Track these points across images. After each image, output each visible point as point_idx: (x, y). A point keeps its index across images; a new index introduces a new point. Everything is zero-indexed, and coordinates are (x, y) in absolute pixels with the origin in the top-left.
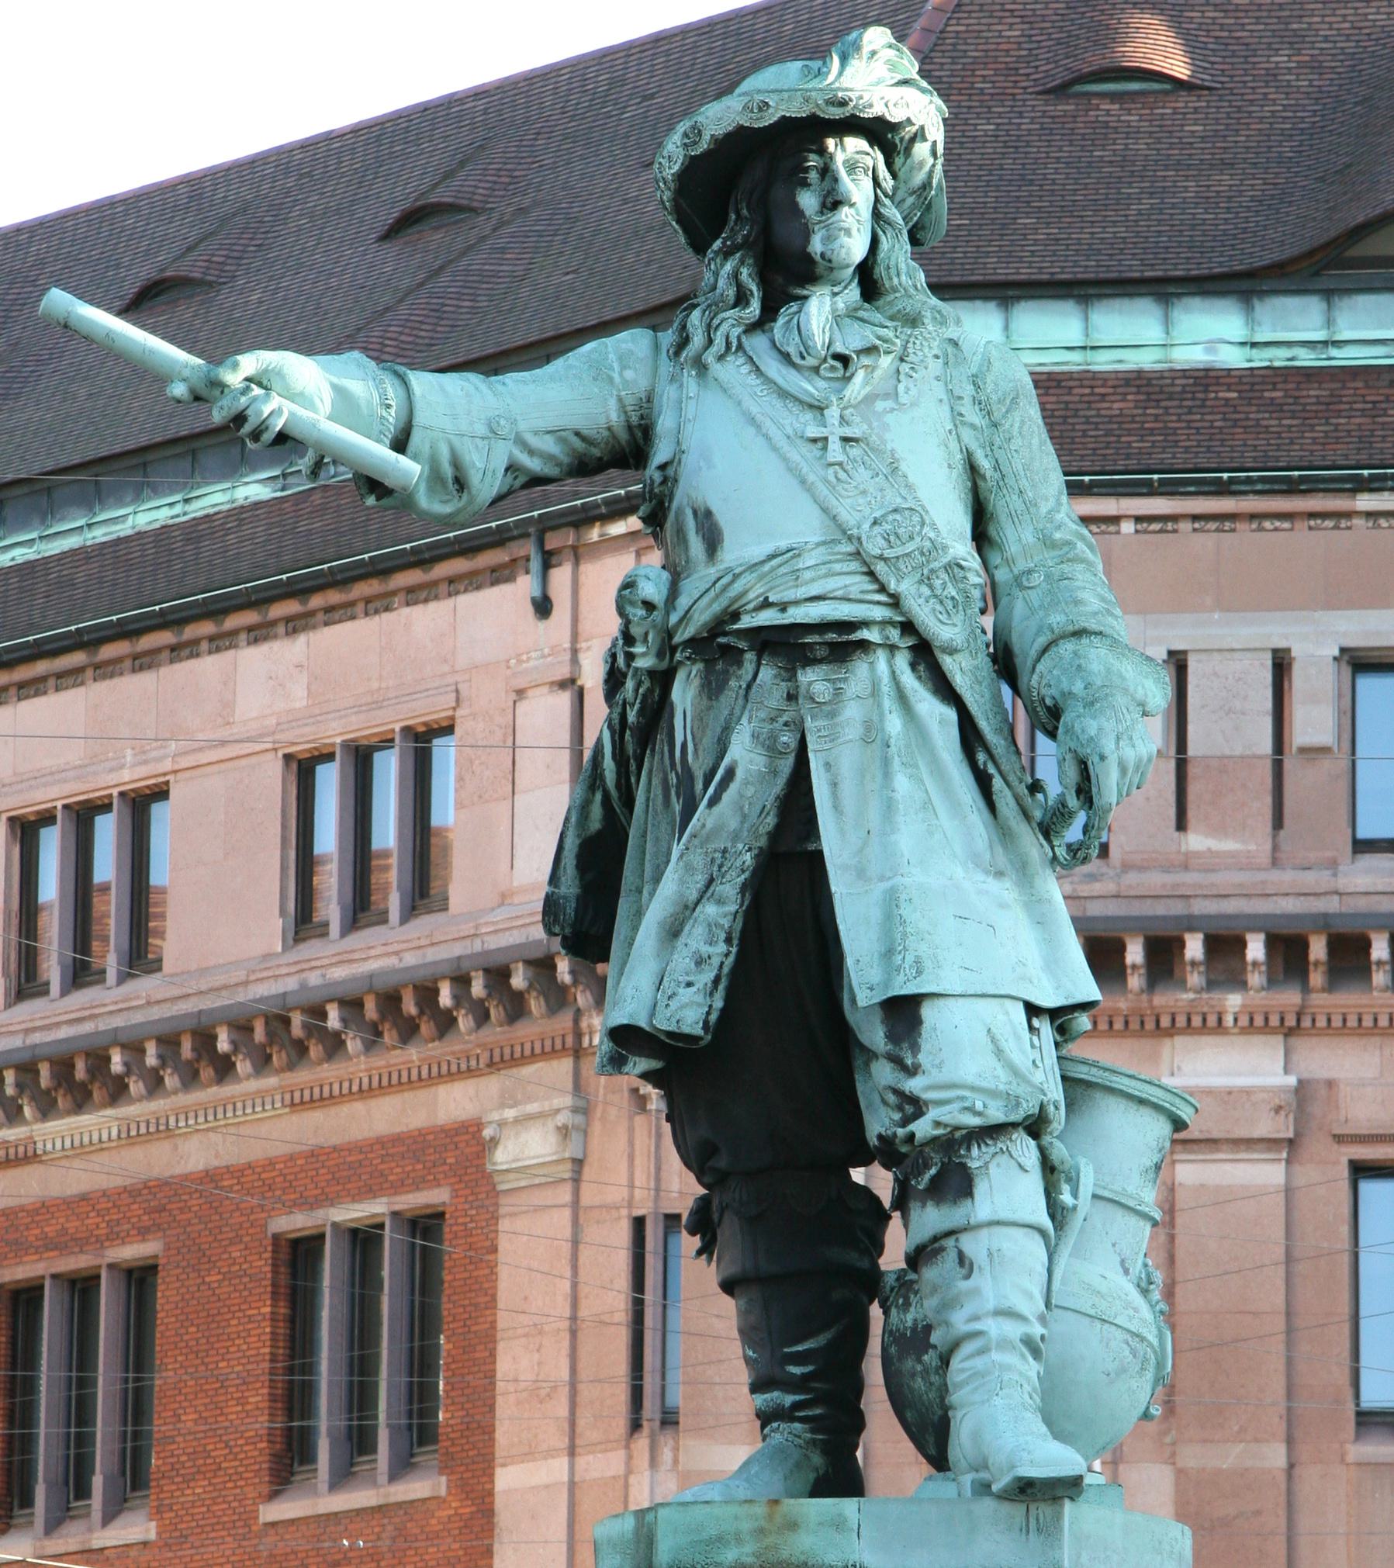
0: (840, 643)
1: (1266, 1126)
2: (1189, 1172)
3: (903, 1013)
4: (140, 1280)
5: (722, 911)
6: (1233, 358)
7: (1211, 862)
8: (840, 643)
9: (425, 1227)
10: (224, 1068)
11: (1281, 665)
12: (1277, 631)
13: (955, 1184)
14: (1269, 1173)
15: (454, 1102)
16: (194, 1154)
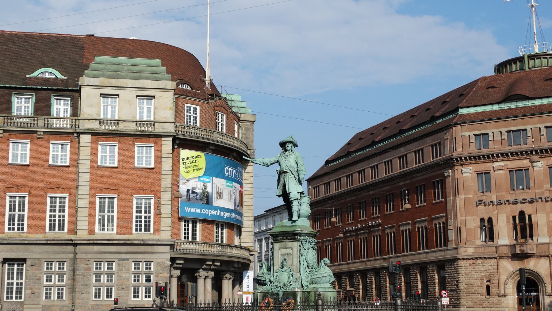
0: (287, 172)
1: (502, 168)
2: (496, 172)
3: (289, 193)
4: (424, 185)
5: (282, 188)
6: (498, 109)
7: (497, 148)
8: (287, 172)
9: (441, 180)
10: (428, 169)
11: (501, 132)
12: (500, 130)
13: (292, 203)
14: (502, 172)
15: (442, 171)
16: (426, 176)
